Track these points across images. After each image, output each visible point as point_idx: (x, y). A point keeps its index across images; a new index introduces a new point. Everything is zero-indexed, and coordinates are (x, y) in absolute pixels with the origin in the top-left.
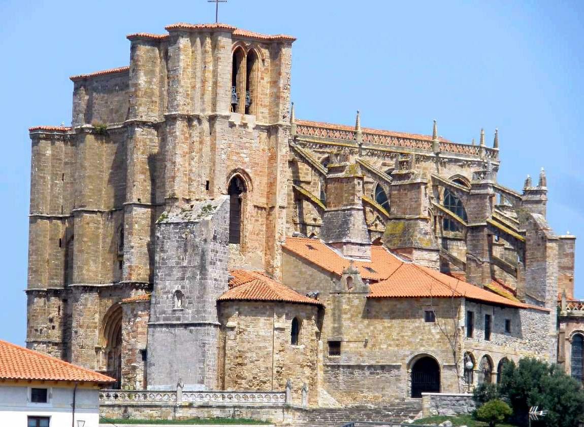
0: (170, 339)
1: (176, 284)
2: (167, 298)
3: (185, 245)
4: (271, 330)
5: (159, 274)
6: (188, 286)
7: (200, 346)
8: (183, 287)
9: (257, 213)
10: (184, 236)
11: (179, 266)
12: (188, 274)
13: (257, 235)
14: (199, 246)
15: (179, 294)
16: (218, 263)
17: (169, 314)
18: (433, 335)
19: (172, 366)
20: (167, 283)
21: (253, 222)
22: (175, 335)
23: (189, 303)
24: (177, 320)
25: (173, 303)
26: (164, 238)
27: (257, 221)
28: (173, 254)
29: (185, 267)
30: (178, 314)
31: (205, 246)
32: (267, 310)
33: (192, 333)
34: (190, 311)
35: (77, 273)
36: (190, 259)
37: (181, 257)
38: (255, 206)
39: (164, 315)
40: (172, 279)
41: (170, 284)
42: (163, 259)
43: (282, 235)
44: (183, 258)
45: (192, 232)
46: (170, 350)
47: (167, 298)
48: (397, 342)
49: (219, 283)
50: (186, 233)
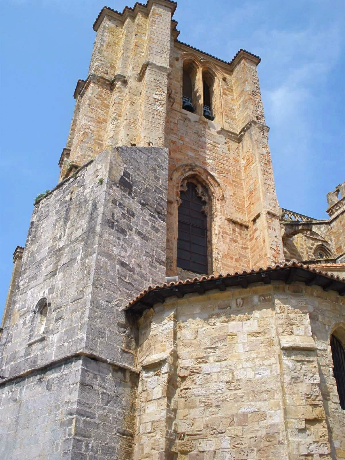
4: (273, 360)
8: (52, 290)
9: (234, 230)
12: (64, 260)
13: (237, 260)
16: (136, 238)
20: (29, 293)
21: (228, 240)
25: (31, 331)
27: (235, 241)
32: (253, 308)
36: (71, 230)
38: (230, 220)
39: (13, 363)
41: (32, 295)
43: (278, 253)
49: (136, 277)
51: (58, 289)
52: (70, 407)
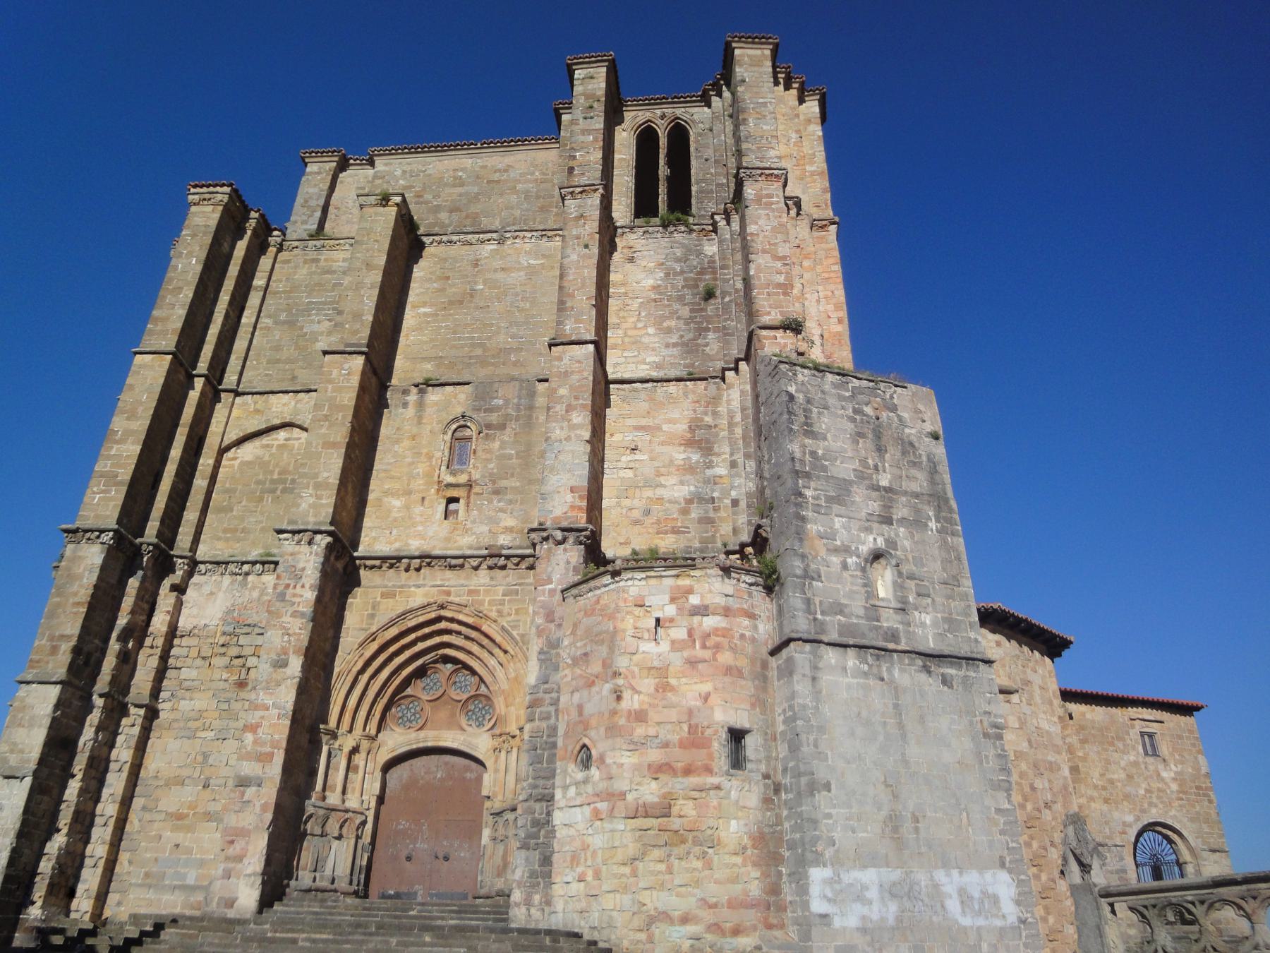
0: (879, 700)
1: (868, 530)
2: (845, 566)
3: (878, 436)
5: (808, 493)
6: (906, 543)
7: (986, 735)
10: (868, 410)
11: (867, 482)
14: (916, 445)
15: (877, 556)
17: (858, 617)
18: (1166, 784)
19: (895, 796)
20: (838, 523)
22: (897, 690)
23: (919, 595)
24: (886, 641)
25: (865, 585)
26: (809, 401)
28: (846, 451)
29: (888, 490)
30: (890, 620)
31: (934, 450)
33: (951, 687)
34: (927, 619)
35: (311, 500)
37: (870, 461)
39: (839, 617)
40: (851, 515)
42: (813, 454)
44: (876, 467)
45: (893, 408)
46: (881, 738)
47: (845, 566)
48: (1104, 793)
50: (876, 406)
51: (905, 550)
52: (992, 719)
